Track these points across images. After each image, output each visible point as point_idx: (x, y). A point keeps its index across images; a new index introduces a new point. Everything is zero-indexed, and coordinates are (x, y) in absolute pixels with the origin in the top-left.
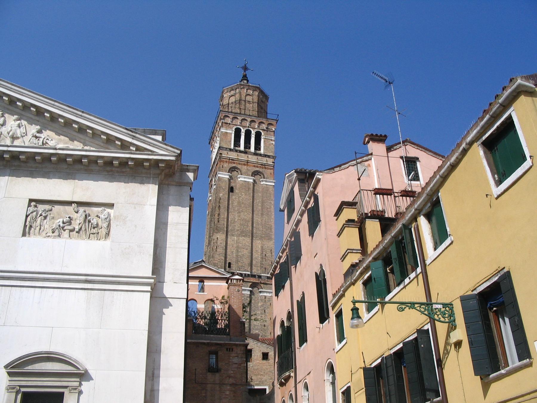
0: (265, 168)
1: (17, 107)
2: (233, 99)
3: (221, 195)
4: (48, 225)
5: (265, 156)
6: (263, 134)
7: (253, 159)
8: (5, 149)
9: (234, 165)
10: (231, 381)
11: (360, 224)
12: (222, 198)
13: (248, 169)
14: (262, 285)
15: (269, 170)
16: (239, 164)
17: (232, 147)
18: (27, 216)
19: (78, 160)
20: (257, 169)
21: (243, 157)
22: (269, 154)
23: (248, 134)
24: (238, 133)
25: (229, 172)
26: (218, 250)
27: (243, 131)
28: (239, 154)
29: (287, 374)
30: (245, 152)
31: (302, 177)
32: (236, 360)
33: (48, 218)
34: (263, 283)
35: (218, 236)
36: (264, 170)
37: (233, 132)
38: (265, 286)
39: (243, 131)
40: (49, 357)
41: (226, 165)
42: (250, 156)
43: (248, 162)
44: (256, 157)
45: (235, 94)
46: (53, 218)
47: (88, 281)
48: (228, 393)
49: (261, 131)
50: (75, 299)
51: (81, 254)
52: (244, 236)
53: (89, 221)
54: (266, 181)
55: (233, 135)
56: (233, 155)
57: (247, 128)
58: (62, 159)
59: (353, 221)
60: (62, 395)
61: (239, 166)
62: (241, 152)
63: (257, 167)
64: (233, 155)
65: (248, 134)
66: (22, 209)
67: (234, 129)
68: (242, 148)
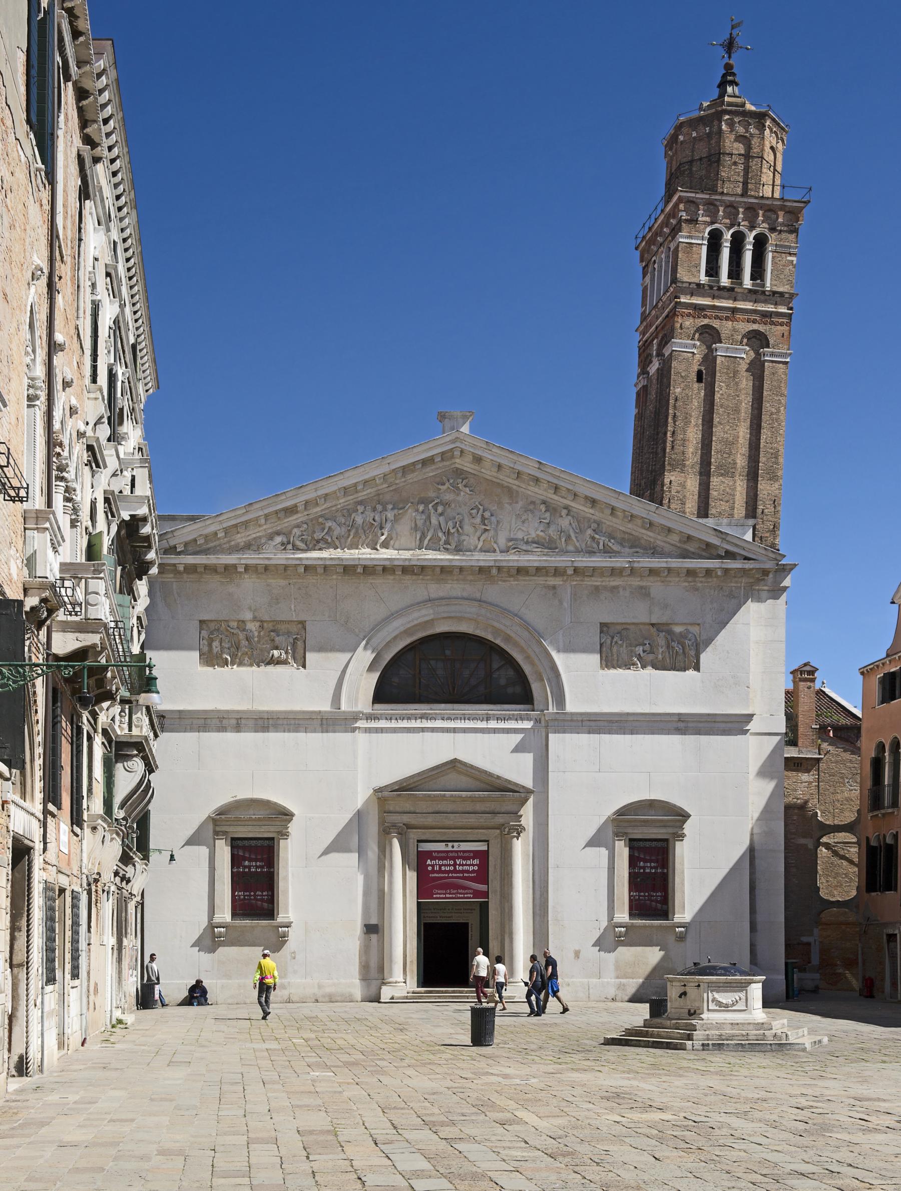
0: (772, 323)
2: (702, 150)
3: (678, 390)
9: (706, 321)
12: (680, 397)
13: (735, 330)
15: (779, 327)
16: (717, 317)
17: (703, 279)
20: (755, 327)
22: (781, 289)
24: (715, 240)
25: (693, 339)
35: (673, 478)
36: (768, 327)
37: (706, 242)
40: (651, 805)
41: (688, 322)
43: (734, 310)
45: (709, 135)
52: (722, 475)
54: (772, 354)
55: (704, 249)
61: (716, 324)
63: (754, 322)
68: (725, 280)
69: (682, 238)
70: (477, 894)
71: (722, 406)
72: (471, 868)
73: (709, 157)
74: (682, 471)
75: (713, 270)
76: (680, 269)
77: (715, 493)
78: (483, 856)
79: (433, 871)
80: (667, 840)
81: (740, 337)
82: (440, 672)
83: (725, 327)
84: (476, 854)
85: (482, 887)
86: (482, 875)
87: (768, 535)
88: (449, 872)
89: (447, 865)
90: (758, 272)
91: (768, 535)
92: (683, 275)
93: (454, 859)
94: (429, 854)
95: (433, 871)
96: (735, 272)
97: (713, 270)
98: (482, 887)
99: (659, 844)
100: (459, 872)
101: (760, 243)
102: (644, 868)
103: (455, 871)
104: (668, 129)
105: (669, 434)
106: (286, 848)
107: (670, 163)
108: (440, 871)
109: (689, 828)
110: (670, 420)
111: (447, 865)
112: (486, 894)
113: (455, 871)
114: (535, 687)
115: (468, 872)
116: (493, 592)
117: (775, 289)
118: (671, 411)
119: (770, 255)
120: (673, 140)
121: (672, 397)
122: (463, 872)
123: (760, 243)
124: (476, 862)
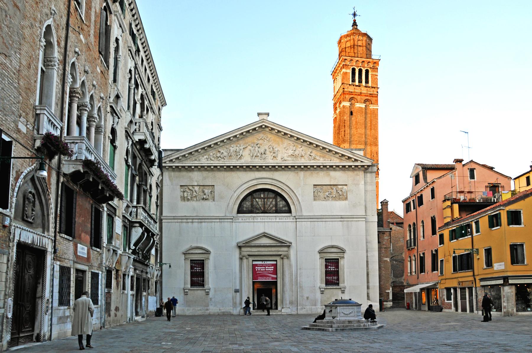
2: (348, 44)
6: (370, 71)
9: (352, 96)
11: (451, 207)
17: (351, 83)
21: (358, 90)
23: (360, 71)
24: (354, 70)
30: (360, 86)
32: (386, 238)
40: (333, 247)
41: (347, 96)
45: (350, 40)
50: (338, 225)
51: (338, 207)
53: (338, 193)
60: (338, 259)
61: (356, 97)
62: (357, 86)
65: (360, 71)
66: (312, 189)
70: (273, 278)
75: (353, 80)
78: (275, 266)
79: (258, 271)
80: (338, 259)
82: (260, 203)
84: (273, 265)
85: (275, 276)
86: (275, 272)
89: (263, 269)
90: (367, 82)
93: (265, 266)
94: (256, 265)
95: (258, 271)
96: (360, 81)
97: (353, 80)
98: (275, 276)
101: (367, 72)
103: (265, 271)
104: (338, 39)
106: (208, 263)
107: (339, 48)
108: (260, 271)
109: (346, 255)
111: (263, 269)
112: (276, 278)
113: (265, 271)
114: (292, 207)
116: (277, 175)
120: (340, 42)
123: (367, 72)
124: (273, 267)
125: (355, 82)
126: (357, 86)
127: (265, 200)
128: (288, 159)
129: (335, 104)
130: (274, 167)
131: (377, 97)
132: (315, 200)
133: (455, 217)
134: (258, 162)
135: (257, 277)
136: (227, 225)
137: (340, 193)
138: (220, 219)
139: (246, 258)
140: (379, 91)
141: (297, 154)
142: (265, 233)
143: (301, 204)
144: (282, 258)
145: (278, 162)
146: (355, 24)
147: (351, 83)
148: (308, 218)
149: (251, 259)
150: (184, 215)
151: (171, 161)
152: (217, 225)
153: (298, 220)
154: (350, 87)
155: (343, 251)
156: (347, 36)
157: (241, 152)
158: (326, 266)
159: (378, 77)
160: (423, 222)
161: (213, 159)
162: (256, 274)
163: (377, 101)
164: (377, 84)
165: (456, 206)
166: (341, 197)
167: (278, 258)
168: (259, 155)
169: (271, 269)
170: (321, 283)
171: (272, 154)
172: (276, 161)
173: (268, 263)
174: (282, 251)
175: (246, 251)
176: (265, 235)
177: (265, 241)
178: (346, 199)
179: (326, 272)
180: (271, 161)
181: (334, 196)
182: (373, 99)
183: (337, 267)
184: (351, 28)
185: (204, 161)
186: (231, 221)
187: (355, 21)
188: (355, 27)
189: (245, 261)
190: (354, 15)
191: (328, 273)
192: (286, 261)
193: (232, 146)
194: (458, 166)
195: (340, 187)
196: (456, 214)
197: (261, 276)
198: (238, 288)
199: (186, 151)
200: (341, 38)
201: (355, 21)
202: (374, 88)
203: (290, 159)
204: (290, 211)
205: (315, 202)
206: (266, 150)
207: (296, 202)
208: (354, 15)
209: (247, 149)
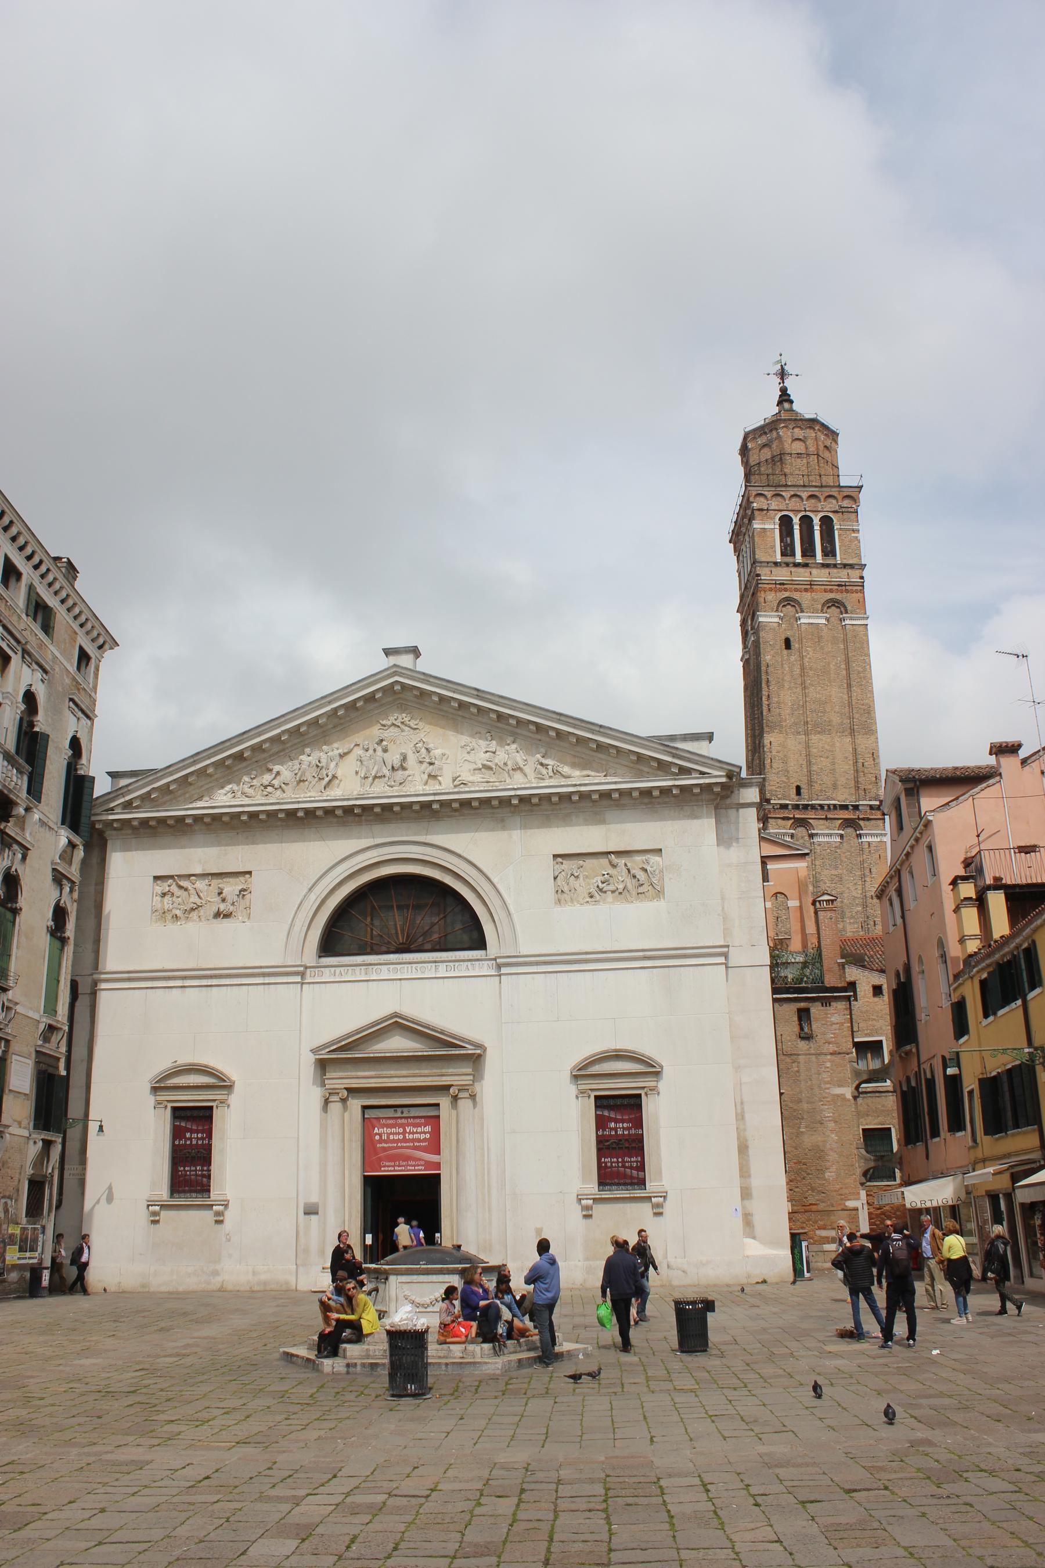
0: (847, 591)
1: (509, 725)
2: (766, 454)
3: (768, 658)
4: (583, 887)
5: (845, 566)
6: (835, 521)
7: (820, 575)
8: (512, 793)
9: (787, 594)
10: (832, 1048)
11: (980, 902)
12: (770, 663)
13: (813, 600)
14: (861, 823)
15: (854, 595)
16: (796, 590)
17: (779, 558)
18: (555, 878)
19: (606, 795)
20: (832, 596)
21: (802, 575)
22: (851, 562)
23: (806, 521)
24: (786, 523)
25: (777, 611)
26: (775, 765)
27: (796, 520)
28: (793, 569)
29: (908, 1047)
30: (806, 565)
31: (910, 785)
33: (581, 877)
34: (863, 819)
36: (845, 595)
37: (777, 526)
38: (867, 823)
39: (796, 520)
40: (618, 1056)
42: (814, 571)
43: (811, 584)
44: (827, 571)
46: (587, 877)
47: (647, 955)
48: (828, 1064)
49: (831, 515)
51: (631, 923)
52: (819, 733)
54: (851, 619)
56: (782, 574)
57: (803, 513)
58: (584, 796)
59: (970, 899)
61: (796, 596)
62: (797, 565)
63: (831, 591)
64: (782, 574)
65: (806, 521)
66: (548, 867)
67: (777, 520)
68: (798, 558)
69: (757, 525)
70: (429, 1164)
71: (811, 669)
72: (423, 1136)
73: (773, 457)
74: (781, 732)
75: (788, 550)
76: (757, 552)
77: (815, 750)
78: (435, 1121)
79: (381, 1141)
81: (820, 607)
83: (805, 598)
85: (434, 1158)
87: (871, 787)
88: (398, 1141)
91: (871, 787)
92: (760, 556)
95: (381, 1141)
96: (808, 550)
98: (434, 1158)
99: (632, 1101)
100: (410, 1141)
101: (826, 522)
102: (616, 1129)
103: (405, 1140)
105: (764, 698)
110: (764, 685)
112: (438, 1166)
113: (405, 1140)
115: (419, 1141)
117: (845, 562)
118: (764, 677)
119: (836, 532)
120: (744, 451)
121: (763, 664)
122: (413, 1140)
123: (826, 522)
124: (428, 1129)
125: (793, 554)
126: (797, 565)
127: (406, 912)
128: (471, 779)
129: (743, 623)
130: (426, 806)
131: (862, 591)
132: (559, 901)
133: (996, 935)
134: (380, 793)
135: (380, 1160)
136: (286, 993)
137: (641, 875)
138: (264, 975)
139: (344, 1101)
140: (865, 573)
141: (501, 764)
142: (396, 1015)
143: (515, 917)
144: (455, 1098)
145: (444, 788)
146: (785, 397)
147: (779, 558)
148: (537, 963)
149: (356, 1104)
150: (160, 967)
151: (128, 805)
152: (255, 995)
153: (504, 970)
154: (776, 571)
155: (653, 1070)
156: (761, 431)
157: (332, 765)
158: (601, 1123)
159: (861, 536)
160: (920, 957)
161: (250, 791)
162: (376, 1151)
163: (862, 603)
164: (859, 556)
165: (997, 902)
166: (641, 890)
167: (445, 1102)
168: (386, 771)
169: (424, 1132)
170: (584, 1180)
171: (425, 765)
172: (433, 787)
173: (414, 1112)
174: (455, 1076)
175: (340, 1079)
176: (397, 1024)
177: (398, 1044)
178: (659, 893)
179: (600, 1141)
180: (420, 788)
181: (621, 887)
182: (849, 599)
183: (639, 1123)
184: (776, 410)
185: (224, 799)
186: (298, 979)
187: (784, 391)
188: (786, 405)
189: (335, 1107)
190: (782, 374)
191: (605, 1146)
192: (464, 1104)
193: (308, 750)
194: (1009, 764)
195: (638, 858)
196: (1001, 926)
197: (393, 1158)
198: (314, 1199)
199: (171, 774)
200: (745, 438)
201: (784, 391)
202: (851, 566)
203: (477, 778)
204: (480, 943)
205: (558, 909)
206: (404, 758)
207: (499, 914)
208: (782, 374)
209: (351, 759)
